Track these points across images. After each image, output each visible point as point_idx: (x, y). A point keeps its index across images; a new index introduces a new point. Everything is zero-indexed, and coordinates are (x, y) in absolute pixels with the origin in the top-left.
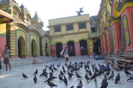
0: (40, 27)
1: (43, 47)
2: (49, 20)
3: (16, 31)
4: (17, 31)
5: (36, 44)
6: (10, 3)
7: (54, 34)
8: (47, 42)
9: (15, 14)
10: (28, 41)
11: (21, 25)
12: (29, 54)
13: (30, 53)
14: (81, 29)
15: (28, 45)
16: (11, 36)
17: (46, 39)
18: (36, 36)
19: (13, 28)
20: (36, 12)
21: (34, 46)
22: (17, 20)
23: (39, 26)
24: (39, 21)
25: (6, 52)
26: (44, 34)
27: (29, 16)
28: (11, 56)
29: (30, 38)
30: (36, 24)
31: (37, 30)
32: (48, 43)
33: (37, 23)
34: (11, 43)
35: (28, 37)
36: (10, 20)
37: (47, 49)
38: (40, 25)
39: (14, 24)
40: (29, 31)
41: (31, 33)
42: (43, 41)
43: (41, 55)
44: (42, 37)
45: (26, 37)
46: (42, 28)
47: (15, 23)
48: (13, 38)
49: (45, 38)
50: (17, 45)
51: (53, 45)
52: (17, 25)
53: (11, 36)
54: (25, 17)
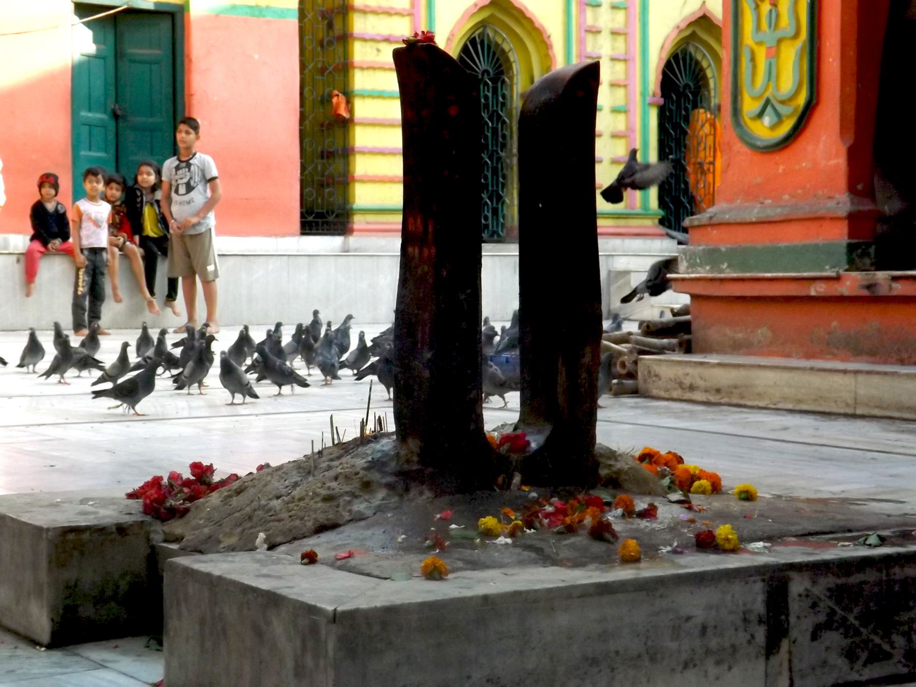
16: (365, 11)
25: (183, 177)
28: (358, 221)
53: (365, 11)
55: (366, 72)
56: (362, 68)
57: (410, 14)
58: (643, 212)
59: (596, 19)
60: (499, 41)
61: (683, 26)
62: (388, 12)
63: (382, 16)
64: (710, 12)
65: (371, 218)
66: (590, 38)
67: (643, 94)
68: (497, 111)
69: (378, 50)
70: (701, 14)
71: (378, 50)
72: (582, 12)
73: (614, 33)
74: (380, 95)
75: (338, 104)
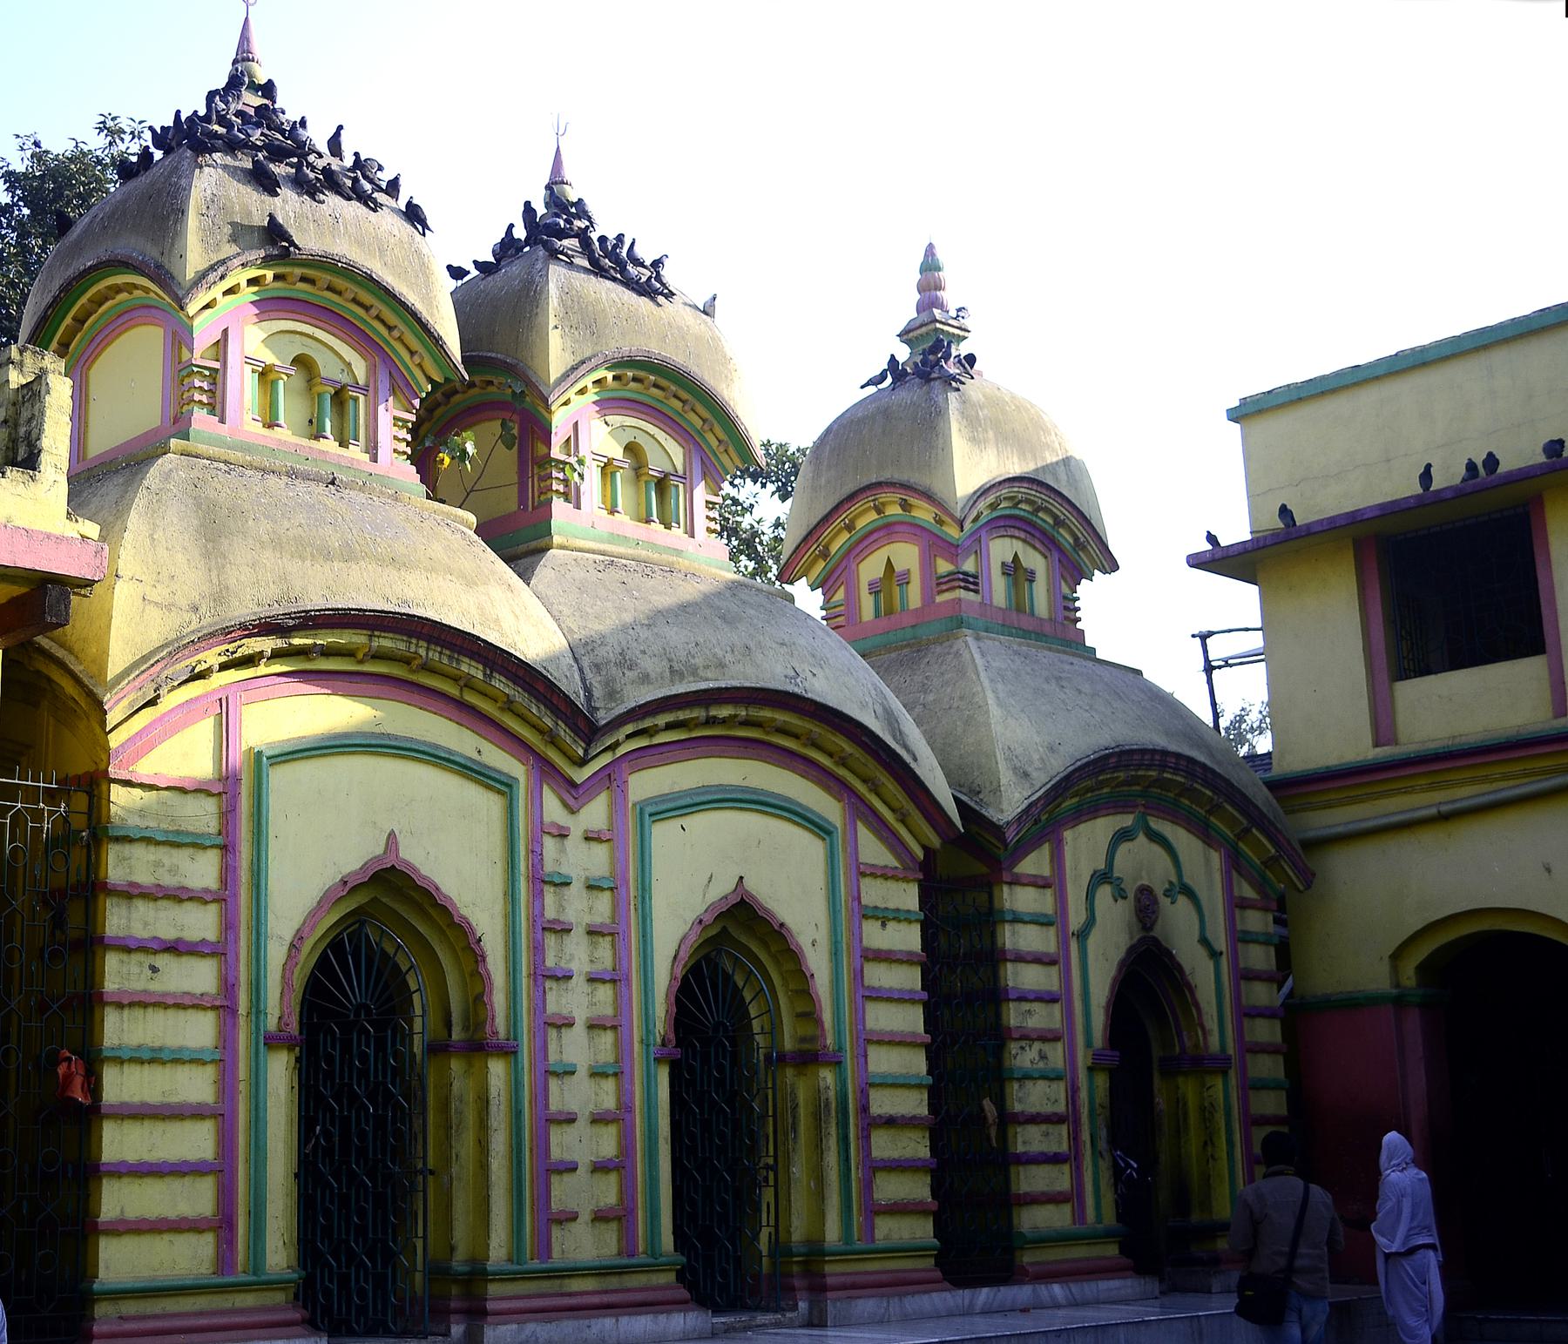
0: (999, 589)
1: (1024, 1057)
2: (1246, 413)
3: (237, 792)
4: (278, 778)
5: (809, 1015)
6: (192, 221)
7: (1383, 729)
8: (1180, 928)
9: (335, 407)
10: (576, 954)
11: (386, 642)
12: (582, 1244)
13: (617, 1216)
14: (1402, 679)
15: (575, 1048)
16: (131, 893)
17: (1142, 861)
18: (820, 828)
19: (189, 713)
20: (930, 265)
21: (779, 1060)
22: (277, 544)
23: (970, 582)
24: (972, 467)
26: (1059, 765)
27: (668, 394)
29: (627, 888)
30: (916, 531)
31: (848, 683)
32: (1202, 973)
33: (924, 513)
34: (117, 1030)
35: (579, 860)
36: (17, 590)
37: (1189, 1088)
38: (1002, 549)
39: (176, 648)
40: (589, 730)
41: (646, 784)
42: (1042, 921)
43: (975, 1239)
44: (996, 830)
45: (530, 877)
46: (1068, 610)
47: (208, 621)
48: (168, 934)
49: (1086, 843)
50: (280, 1071)
51: (1353, 1005)
52: (277, 655)
53: (131, 893)
54: (586, 429)
55: (126, 1012)
56: (120, 1006)
57: (219, 900)
58: (651, 1260)
59: (561, 908)
60: (391, 951)
61: (708, 919)
62: (179, 895)
63: (162, 903)
64: (752, 896)
65: (130, 1307)
66: (550, 940)
67: (645, 1043)
68: (385, 1084)
69: (154, 969)
70: (736, 899)
71: (154, 969)
72: (537, 895)
73: (593, 932)
74: (155, 1058)
75: (69, 1077)
